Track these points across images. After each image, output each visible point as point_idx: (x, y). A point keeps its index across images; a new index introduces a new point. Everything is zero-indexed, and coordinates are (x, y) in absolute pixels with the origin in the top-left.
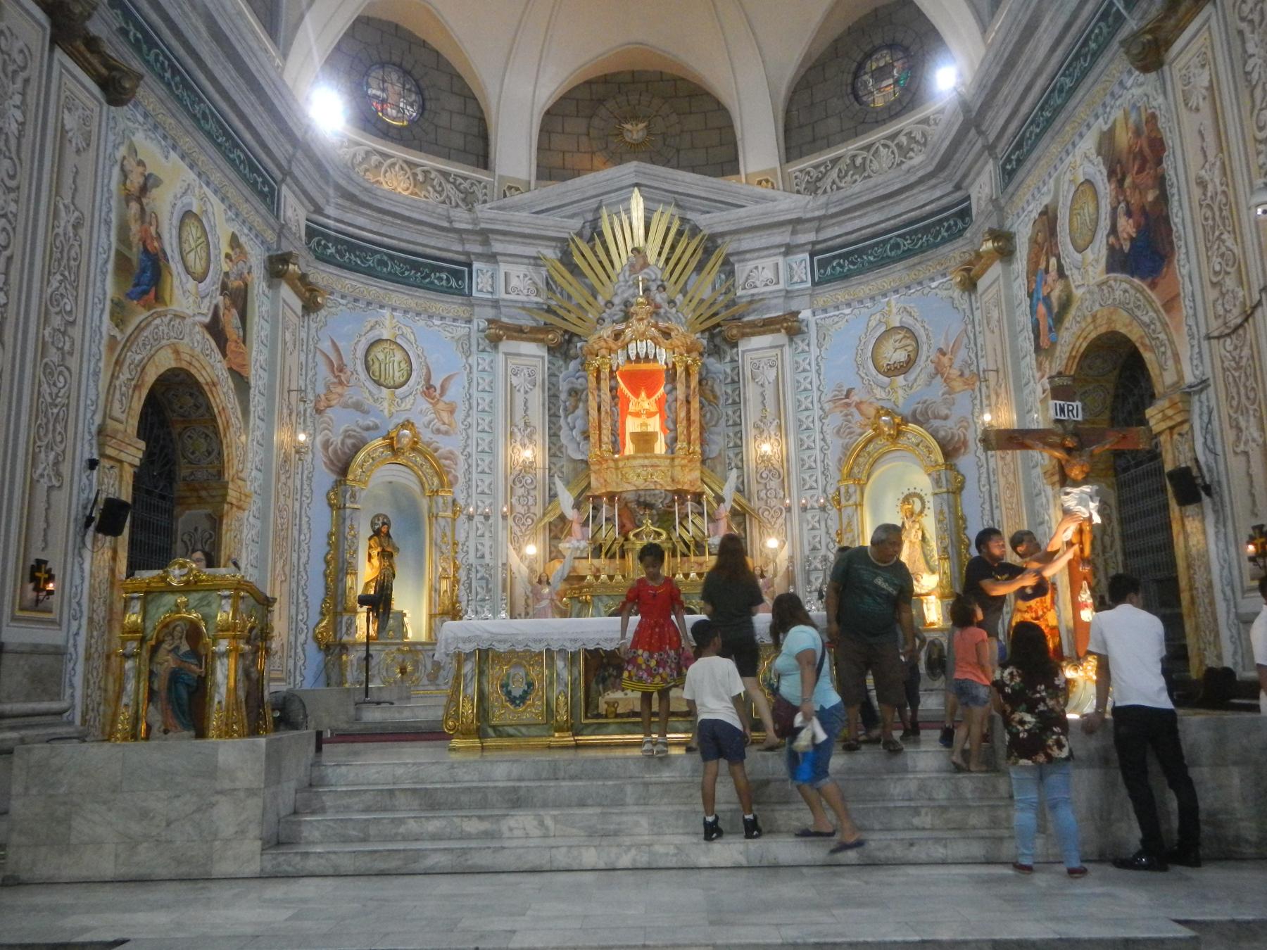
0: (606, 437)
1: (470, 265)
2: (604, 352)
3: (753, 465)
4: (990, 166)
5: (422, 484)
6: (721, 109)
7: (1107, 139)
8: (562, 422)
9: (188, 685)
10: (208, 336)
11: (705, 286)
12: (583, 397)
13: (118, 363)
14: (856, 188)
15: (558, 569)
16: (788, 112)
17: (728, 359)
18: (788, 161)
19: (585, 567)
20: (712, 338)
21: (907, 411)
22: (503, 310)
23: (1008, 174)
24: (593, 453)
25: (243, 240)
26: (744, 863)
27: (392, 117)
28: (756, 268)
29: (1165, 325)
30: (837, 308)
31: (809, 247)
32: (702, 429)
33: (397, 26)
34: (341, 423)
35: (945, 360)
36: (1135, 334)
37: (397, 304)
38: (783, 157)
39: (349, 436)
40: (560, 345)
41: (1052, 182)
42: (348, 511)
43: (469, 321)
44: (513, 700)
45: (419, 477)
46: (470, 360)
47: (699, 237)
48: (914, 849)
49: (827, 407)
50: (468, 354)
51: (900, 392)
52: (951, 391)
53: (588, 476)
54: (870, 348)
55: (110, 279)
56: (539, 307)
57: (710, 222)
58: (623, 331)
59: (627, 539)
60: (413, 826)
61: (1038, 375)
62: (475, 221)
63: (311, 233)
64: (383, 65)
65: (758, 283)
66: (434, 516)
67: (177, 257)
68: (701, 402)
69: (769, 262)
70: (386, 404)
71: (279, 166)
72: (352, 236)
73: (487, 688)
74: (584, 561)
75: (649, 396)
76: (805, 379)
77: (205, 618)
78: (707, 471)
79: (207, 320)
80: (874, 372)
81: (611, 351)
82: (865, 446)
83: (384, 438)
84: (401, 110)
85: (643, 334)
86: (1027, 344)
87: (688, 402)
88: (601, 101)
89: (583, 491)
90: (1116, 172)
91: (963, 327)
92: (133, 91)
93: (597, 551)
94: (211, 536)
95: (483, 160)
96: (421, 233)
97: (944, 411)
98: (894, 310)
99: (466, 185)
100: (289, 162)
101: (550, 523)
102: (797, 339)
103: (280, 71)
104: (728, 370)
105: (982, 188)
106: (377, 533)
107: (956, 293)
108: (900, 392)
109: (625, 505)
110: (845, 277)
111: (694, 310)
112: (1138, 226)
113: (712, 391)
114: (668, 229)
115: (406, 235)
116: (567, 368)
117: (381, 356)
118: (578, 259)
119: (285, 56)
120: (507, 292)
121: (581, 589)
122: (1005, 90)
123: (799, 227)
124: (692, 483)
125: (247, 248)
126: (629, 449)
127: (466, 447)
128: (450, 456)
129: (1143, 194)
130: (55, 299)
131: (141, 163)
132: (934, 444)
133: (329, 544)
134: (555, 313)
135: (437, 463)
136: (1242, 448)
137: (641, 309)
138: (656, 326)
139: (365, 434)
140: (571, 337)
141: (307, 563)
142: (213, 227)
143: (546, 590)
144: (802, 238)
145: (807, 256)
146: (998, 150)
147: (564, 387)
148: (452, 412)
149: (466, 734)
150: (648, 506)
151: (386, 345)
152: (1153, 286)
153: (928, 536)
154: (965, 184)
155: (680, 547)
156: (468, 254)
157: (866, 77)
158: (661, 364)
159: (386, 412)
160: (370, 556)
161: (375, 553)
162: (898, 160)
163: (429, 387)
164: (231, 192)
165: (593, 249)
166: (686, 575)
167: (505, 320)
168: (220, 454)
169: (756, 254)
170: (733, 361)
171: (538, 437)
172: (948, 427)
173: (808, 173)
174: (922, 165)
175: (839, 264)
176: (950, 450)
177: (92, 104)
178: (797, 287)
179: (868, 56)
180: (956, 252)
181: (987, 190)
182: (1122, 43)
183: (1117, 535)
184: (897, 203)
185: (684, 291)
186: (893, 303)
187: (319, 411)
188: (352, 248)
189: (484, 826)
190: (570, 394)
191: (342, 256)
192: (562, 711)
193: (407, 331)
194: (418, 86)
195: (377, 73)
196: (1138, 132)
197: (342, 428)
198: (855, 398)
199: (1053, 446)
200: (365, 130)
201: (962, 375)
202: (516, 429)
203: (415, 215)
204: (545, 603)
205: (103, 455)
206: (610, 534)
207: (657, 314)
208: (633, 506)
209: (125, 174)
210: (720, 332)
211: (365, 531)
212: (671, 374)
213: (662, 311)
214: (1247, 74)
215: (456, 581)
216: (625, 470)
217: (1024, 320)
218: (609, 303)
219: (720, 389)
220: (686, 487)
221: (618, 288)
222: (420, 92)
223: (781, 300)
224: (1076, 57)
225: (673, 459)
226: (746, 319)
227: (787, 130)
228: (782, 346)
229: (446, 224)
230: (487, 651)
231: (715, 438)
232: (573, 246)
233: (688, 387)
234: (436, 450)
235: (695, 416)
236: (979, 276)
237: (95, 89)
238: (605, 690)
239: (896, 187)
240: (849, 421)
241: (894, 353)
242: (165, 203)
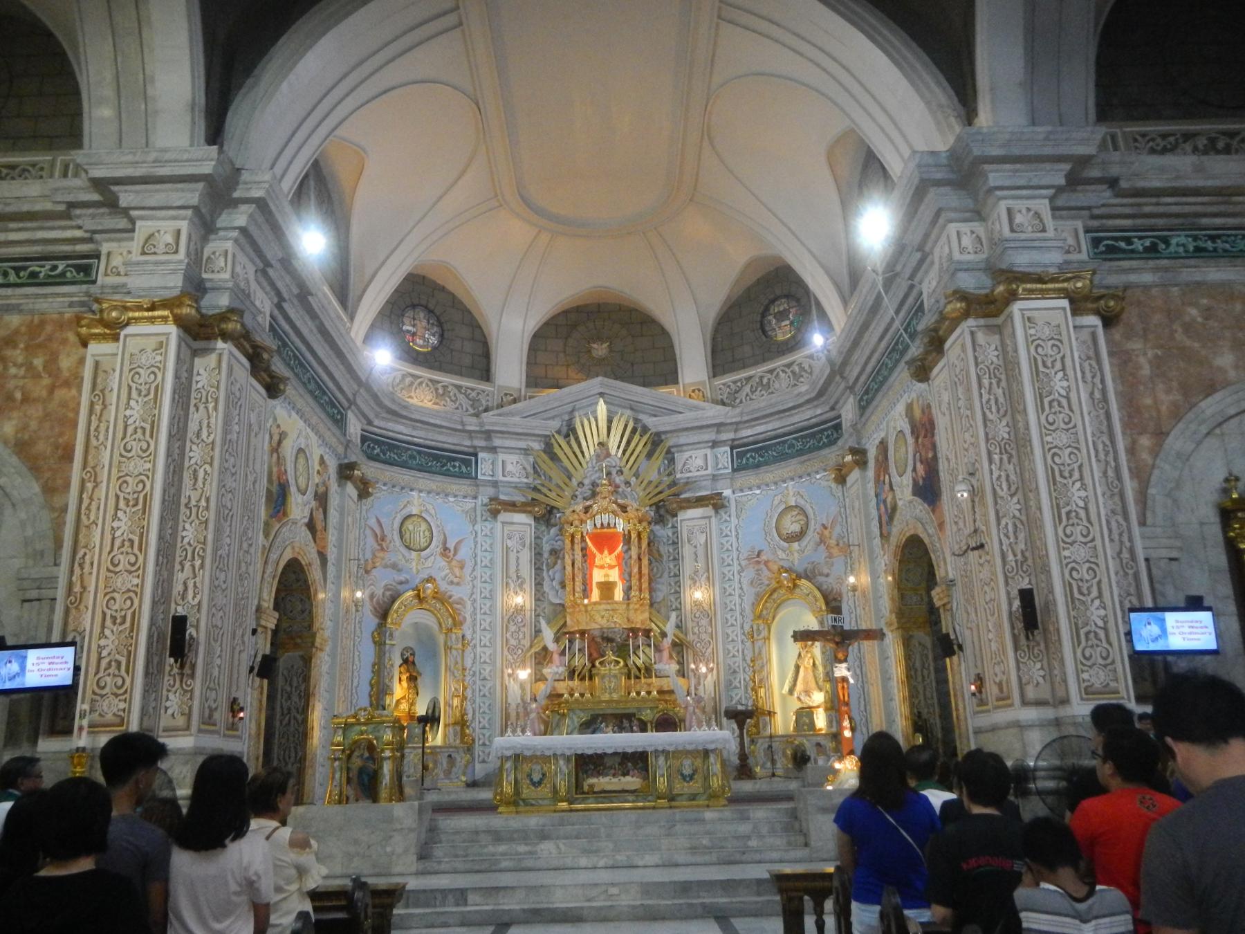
0: (578, 587)
1: (476, 455)
2: (576, 523)
3: (688, 607)
4: (851, 400)
5: (440, 625)
6: (664, 333)
7: (909, 408)
8: (545, 574)
9: (368, 775)
10: (308, 532)
11: (653, 470)
12: (561, 556)
13: (266, 563)
14: (762, 402)
15: (542, 689)
16: (714, 339)
17: (670, 525)
18: (714, 376)
19: (562, 687)
20: (657, 511)
21: (800, 569)
22: (501, 489)
23: (864, 407)
24: (568, 599)
25: (326, 458)
26: (660, 862)
27: (419, 345)
28: (691, 457)
29: (939, 539)
30: (750, 489)
31: (730, 443)
32: (650, 581)
33: (424, 277)
34: (382, 580)
35: (826, 533)
36: (926, 541)
37: (423, 487)
38: (711, 374)
39: (389, 590)
40: (544, 516)
41: (885, 423)
42: (387, 647)
43: (475, 498)
44: (534, 784)
45: (438, 618)
46: (476, 528)
47: (648, 435)
48: (745, 856)
49: (743, 563)
50: (474, 522)
51: (796, 555)
52: (830, 556)
53: (565, 617)
54: (775, 520)
55: (263, 508)
56: (528, 485)
58: (591, 506)
59: (593, 666)
60: (491, 849)
61: (882, 553)
62: (482, 424)
63: (364, 439)
64: (414, 306)
65: (692, 469)
66: (448, 648)
67: (294, 482)
68: (649, 560)
70: (414, 564)
71: (348, 400)
72: (388, 438)
73: (519, 777)
74: (561, 683)
75: (611, 552)
76: (727, 542)
77: (376, 738)
78: (654, 612)
79: (306, 520)
80: (777, 538)
81: (582, 522)
82: (771, 595)
83: (413, 590)
84: (426, 339)
85: (606, 509)
86: (876, 531)
87: (640, 559)
88: (574, 326)
89: (560, 628)
90: (915, 432)
91: (838, 509)
92: (284, 391)
93: (572, 674)
94: (303, 671)
95: (484, 371)
96: (441, 433)
97: (826, 571)
98: (791, 494)
99: (474, 394)
100: (354, 395)
101: (536, 653)
102: (722, 512)
103: (349, 330)
104: (670, 534)
105: (848, 412)
106: (406, 661)
107: (833, 485)
108: (796, 555)
109: (592, 640)
110: (758, 466)
111: (644, 490)
112: (925, 471)
113: (658, 551)
114: (626, 426)
115: (430, 436)
116: (549, 533)
117: (411, 527)
118: (557, 450)
119: (352, 318)
120: (504, 476)
121: (559, 704)
122: (855, 357)
123: (722, 428)
124: (643, 622)
125: (328, 462)
126: (595, 595)
127: (472, 594)
128: (460, 602)
129: (927, 453)
130: (245, 533)
131: (278, 426)
132: (818, 595)
133: (373, 672)
134: (539, 491)
135: (452, 608)
136: (969, 625)
137: (604, 490)
138: (615, 502)
139: (399, 587)
140: (551, 510)
141: (357, 687)
142: (311, 455)
143: (534, 706)
145: (728, 449)
146: (856, 389)
147: (546, 548)
148: (462, 568)
149: (508, 804)
150: (609, 640)
151: (415, 519)
152: (933, 511)
153: (817, 662)
154: (837, 407)
155: (634, 671)
156: (475, 447)
157: (770, 318)
158: (620, 529)
159: (414, 570)
160: (400, 679)
161: (404, 677)
162: (793, 382)
163: (446, 549)
164: (321, 427)
165: (569, 443)
166: (638, 693)
167: (502, 497)
168: (311, 612)
169: (690, 447)
170: (673, 527)
171: (527, 586)
172: (830, 582)
173: (729, 386)
174: (807, 392)
175: (751, 456)
177: (261, 402)
178: (722, 472)
179: (773, 302)
180: (831, 455)
181: (850, 416)
182: (906, 363)
183: (932, 668)
184: (792, 415)
185: (637, 475)
186: (790, 488)
187: (367, 572)
188: (392, 448)
189: (527, 848)
190: (551, 554)
191: (385, 454)
192: (563, 790)
193: (430, 507)
194: (438, 320)
195: (410, 313)
196: (923, 412)
197: (383, 584)
198: (764, 557)
199: (828, 640)
200: (406, 360)
201: (838, 545)
202: (512, 580)
203: (438, 422)
204: (533, 715)
205: (258, 625)
206: (580, 661)
207: (617, 492)
208: (599, 640)
209: (271, 437)
210: (664, 505)
211: (398, 661)
212: (627, 539)
213: (620, 490)
214: (959, 408)
215: (464, 698)
216: (593, 613)
217: (874, 513)
218: (581, 484)
219: (664, 550)
220: (638, 626)
221: (587, 471)
222: (440, 324)
223: (708, 483)
224: (893, 350)
225: (628, 604)
226: (683, 496)
227: (714, 352)
228: (710, 517)
229: (459, 427)
230: (519, 755)
231: (659, 586)
232: (553, 441)
233: (640, 547)
234: (450, 597)
235: (645, 571)
236: (847, 475)
237: (263, 391)
238: (588, 777)
239: (791, 405)
240: (759, 574)
241: (792, 526)
242: (288, 449)
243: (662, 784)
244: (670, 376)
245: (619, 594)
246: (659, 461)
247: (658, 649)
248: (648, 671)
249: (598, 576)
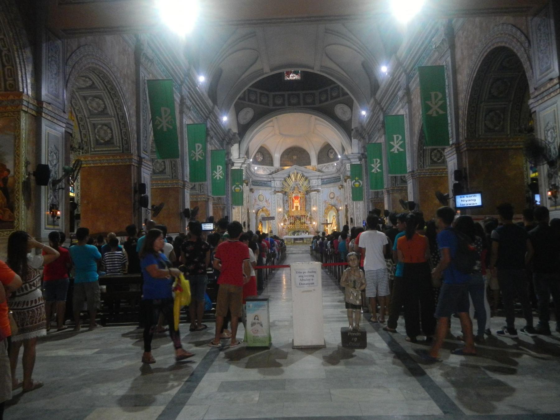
6: (308, 154)
15: (285, 227)
16: (318, 156)
19: (289, 226)
27: (259, 160)
32: (305, 206)
34: (256, 207)
57: (306, 175)
69: (315, 180)
84: (260, 158)
95: (271, 164)
126: (295, 208)
128: (269, 210)
144: (320, 177)
147: (285, 200)
163: (266, 201)
167: (277, 190)
176: (338, 210)
180: (339, 183)
202: (279, 206)
222: (263, 155)
243: (305, 242)
244: (309, 164)
245: (299, 209)
246: (307, 182)
247: (306, 219)
248: (305, 223)
249: (295, 205)
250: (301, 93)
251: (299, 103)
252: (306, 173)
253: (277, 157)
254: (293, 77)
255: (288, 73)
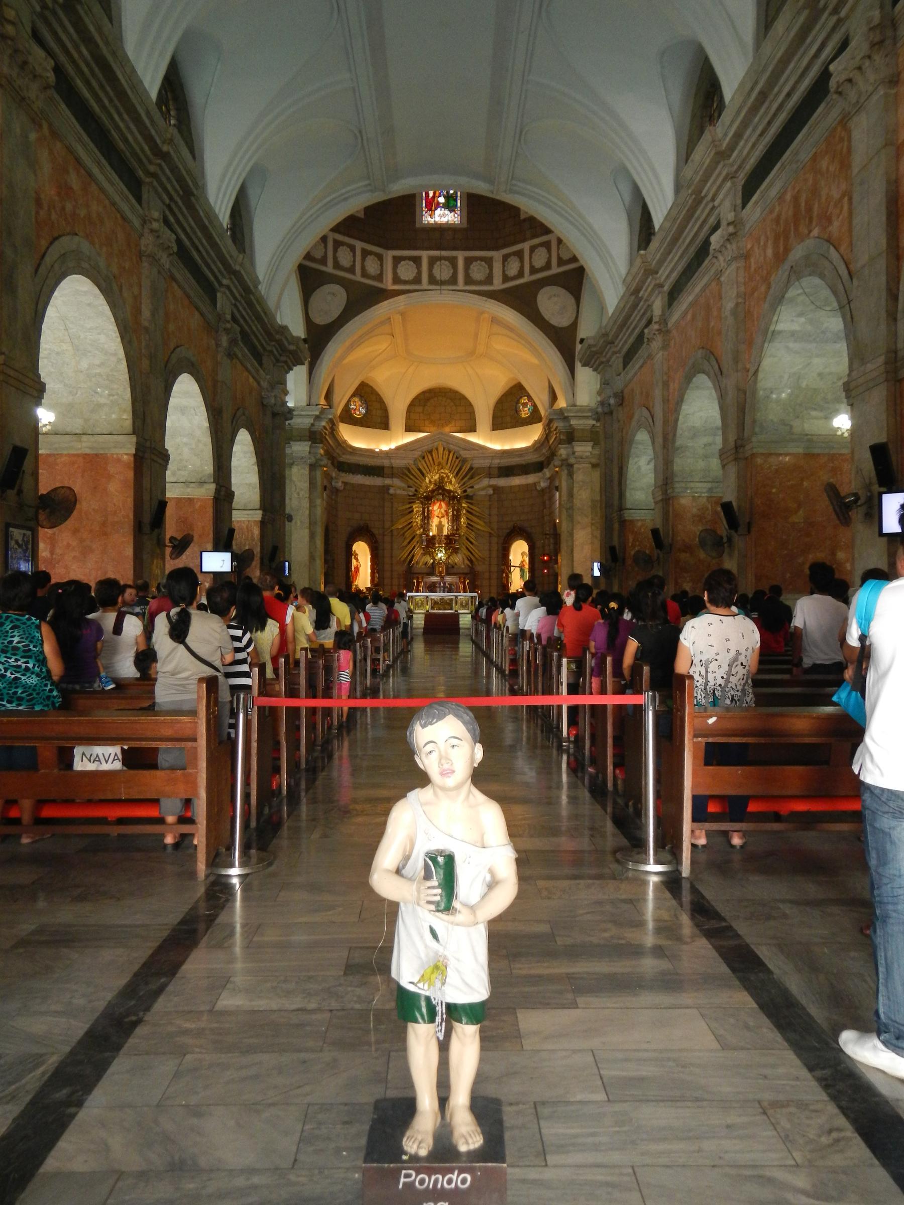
6: (470, 405)
88: (428, 399)
179: (521, 397)
250: (461, 256)
251: (453, 280)
252: (465, 449)
253: (398, 409)
254: (443, 217)
255: (432, 205)
